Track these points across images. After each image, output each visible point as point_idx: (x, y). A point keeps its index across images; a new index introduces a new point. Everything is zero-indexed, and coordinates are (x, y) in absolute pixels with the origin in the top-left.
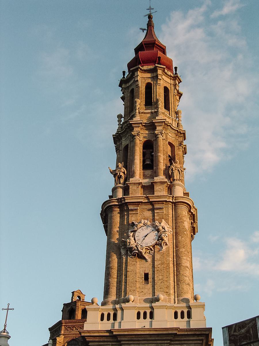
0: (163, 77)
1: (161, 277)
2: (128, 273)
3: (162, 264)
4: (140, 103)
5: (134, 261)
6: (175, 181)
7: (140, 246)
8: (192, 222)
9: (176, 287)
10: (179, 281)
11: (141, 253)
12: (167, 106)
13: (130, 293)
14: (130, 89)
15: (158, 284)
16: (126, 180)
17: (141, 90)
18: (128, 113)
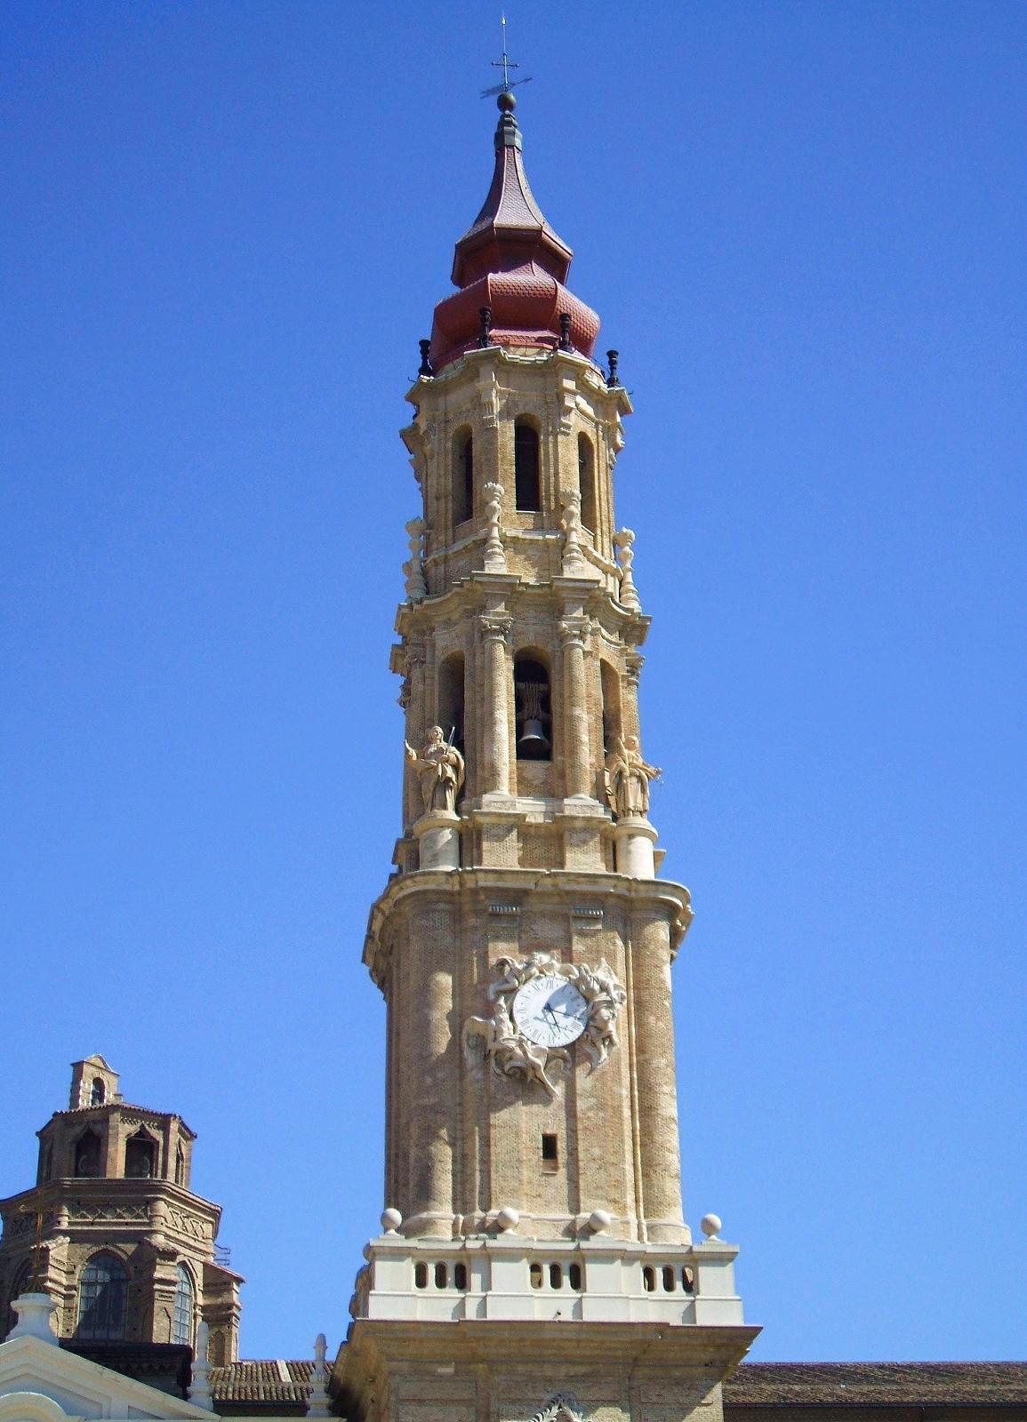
0: (579, 399)
1: (596, 1152)
2: (493, 1131)
3: (601, 1106)
4: (501, 492)
5: (509, 1094)
6: (628, 815)
7: (529, 1043)
8: (672, 955)
9: (640, 1183)
10: (651, 1166)
11: (534, 1067)
12: (588, 520)
13: (502, 1199)
14: (454, 427)
15: (588, 1173)
16: (460, 797)
17: (504, 446)
18: (450, 523)
